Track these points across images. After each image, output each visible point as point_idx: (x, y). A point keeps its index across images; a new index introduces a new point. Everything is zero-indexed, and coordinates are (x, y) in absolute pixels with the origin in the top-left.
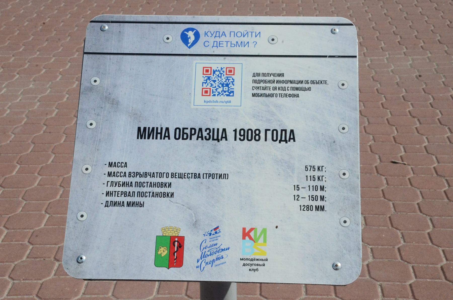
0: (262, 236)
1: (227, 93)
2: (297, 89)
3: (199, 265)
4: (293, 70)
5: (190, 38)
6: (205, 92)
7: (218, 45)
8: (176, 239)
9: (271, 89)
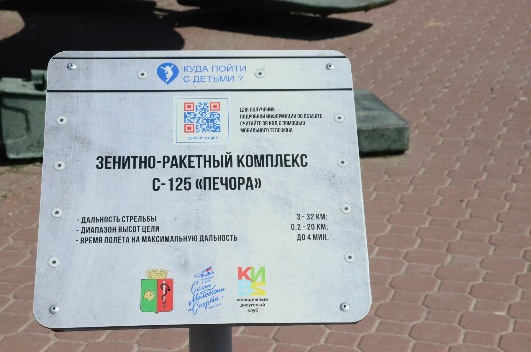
0: (261, 274)
1: (213, 129)
2: (290, 123)
3: (192, 308)
4: (285, 104)
5: (167, 73)
6: (189, 129)
7: (200, 80)
8: (164, 282)
9: (262, 124)
